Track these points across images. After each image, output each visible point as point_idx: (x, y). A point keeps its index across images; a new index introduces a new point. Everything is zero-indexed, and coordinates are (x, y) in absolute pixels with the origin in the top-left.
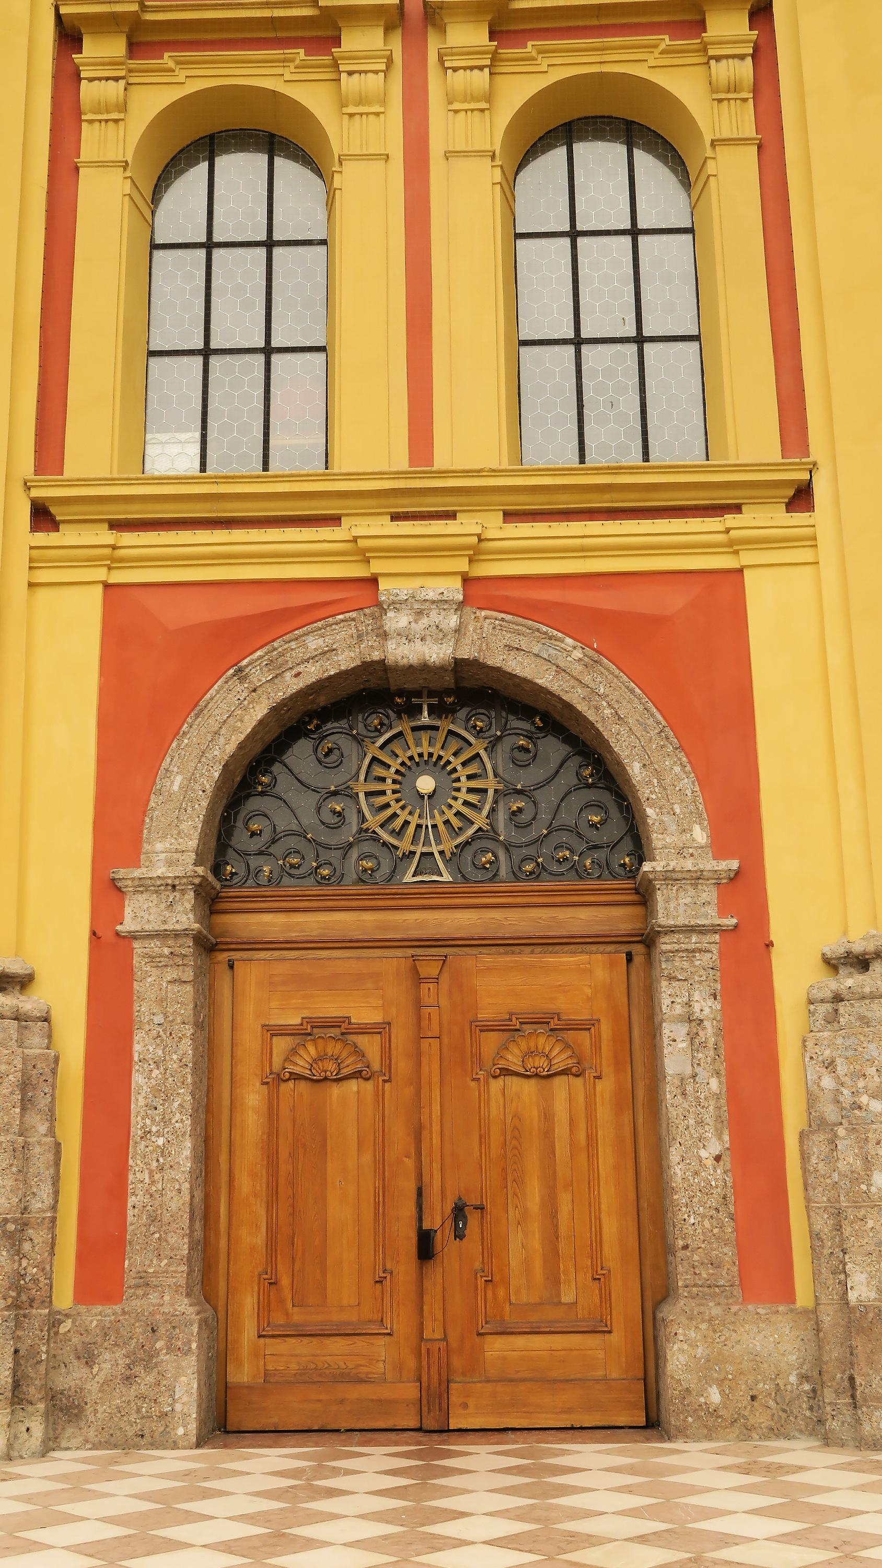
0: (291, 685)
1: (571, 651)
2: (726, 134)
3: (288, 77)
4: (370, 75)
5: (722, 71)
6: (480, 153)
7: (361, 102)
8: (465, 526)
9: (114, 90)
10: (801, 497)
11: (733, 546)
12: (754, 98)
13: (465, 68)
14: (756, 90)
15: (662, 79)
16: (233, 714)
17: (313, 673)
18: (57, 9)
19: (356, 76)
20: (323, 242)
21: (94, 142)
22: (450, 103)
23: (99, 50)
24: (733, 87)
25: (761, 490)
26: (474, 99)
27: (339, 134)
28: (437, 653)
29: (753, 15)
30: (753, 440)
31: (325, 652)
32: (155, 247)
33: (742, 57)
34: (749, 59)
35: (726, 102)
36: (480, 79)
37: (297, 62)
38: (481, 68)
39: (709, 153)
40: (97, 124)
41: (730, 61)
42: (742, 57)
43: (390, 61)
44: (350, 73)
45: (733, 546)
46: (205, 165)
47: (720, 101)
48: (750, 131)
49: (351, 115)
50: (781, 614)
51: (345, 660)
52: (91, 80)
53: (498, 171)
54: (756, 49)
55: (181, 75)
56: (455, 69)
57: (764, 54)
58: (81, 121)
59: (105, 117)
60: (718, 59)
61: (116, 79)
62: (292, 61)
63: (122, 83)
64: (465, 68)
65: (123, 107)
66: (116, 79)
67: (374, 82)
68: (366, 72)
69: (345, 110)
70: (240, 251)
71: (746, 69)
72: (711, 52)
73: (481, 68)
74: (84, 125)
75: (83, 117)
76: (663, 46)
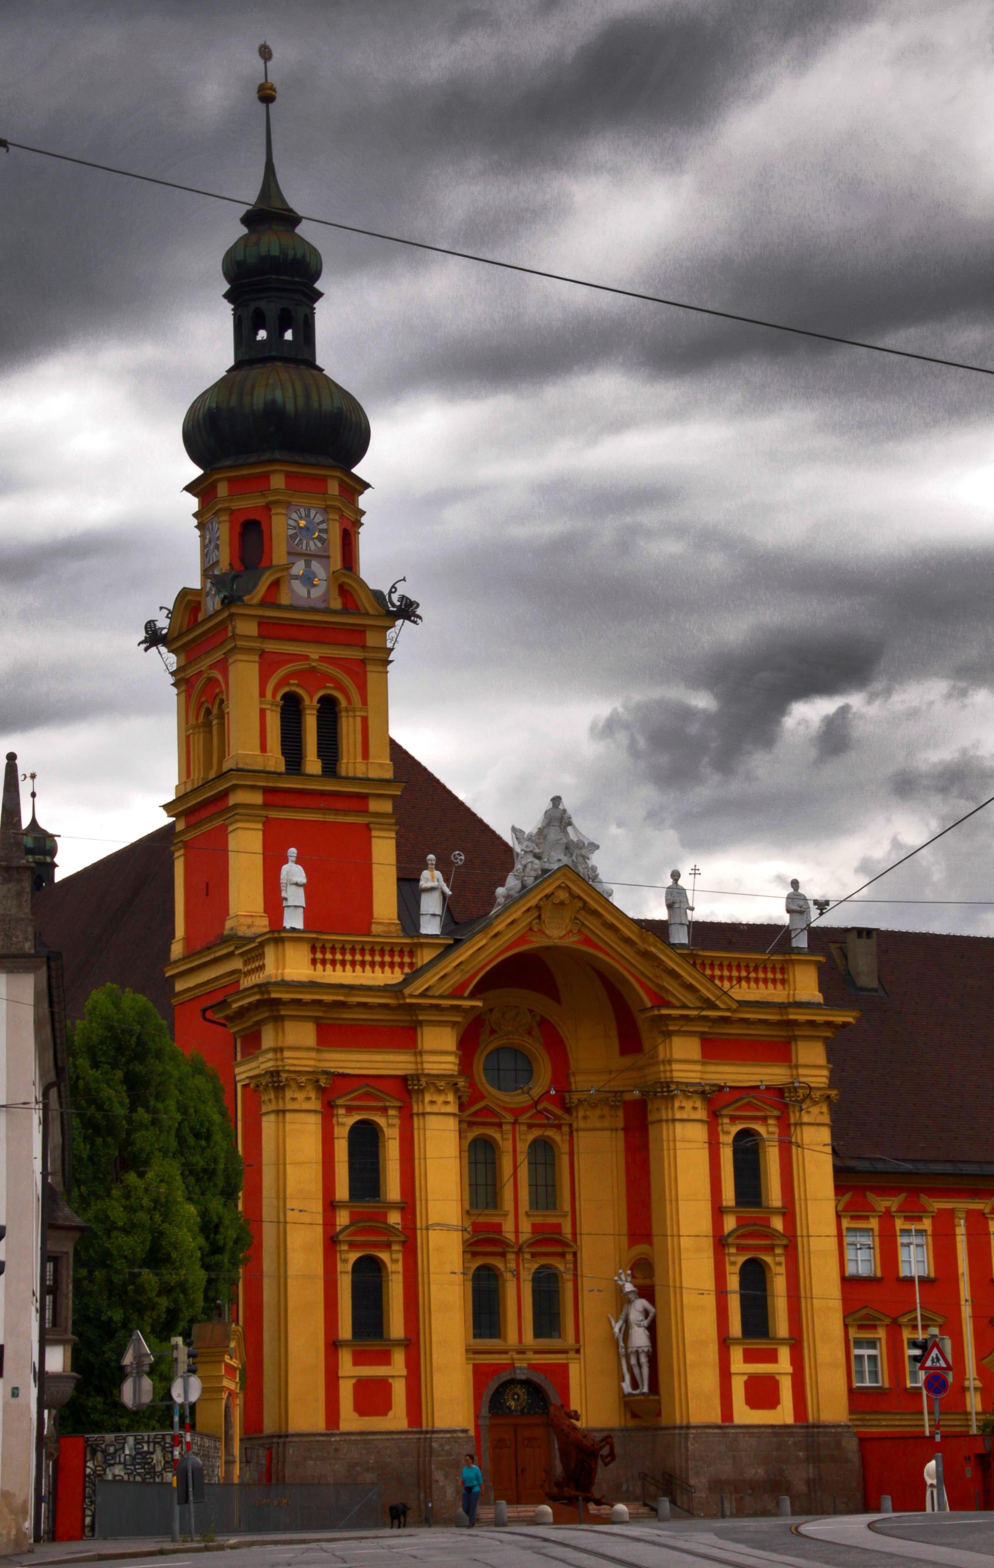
0: (501, 1381)
1: (543, 1377)
8: (530, 1355)
10: (578, 1351)
11: (567, 1359)
15: (558, 1265)
16: (493, 1385)
17: (504, 1379)
25: (571, 1349)
28: (523, 1377)
30: (571, 1339)
31: (505, 1376)
45: (567, 1359)
50: (574, 1371)
51: (509, 1378)
57: (575, 1262)
71: (571, 1266)
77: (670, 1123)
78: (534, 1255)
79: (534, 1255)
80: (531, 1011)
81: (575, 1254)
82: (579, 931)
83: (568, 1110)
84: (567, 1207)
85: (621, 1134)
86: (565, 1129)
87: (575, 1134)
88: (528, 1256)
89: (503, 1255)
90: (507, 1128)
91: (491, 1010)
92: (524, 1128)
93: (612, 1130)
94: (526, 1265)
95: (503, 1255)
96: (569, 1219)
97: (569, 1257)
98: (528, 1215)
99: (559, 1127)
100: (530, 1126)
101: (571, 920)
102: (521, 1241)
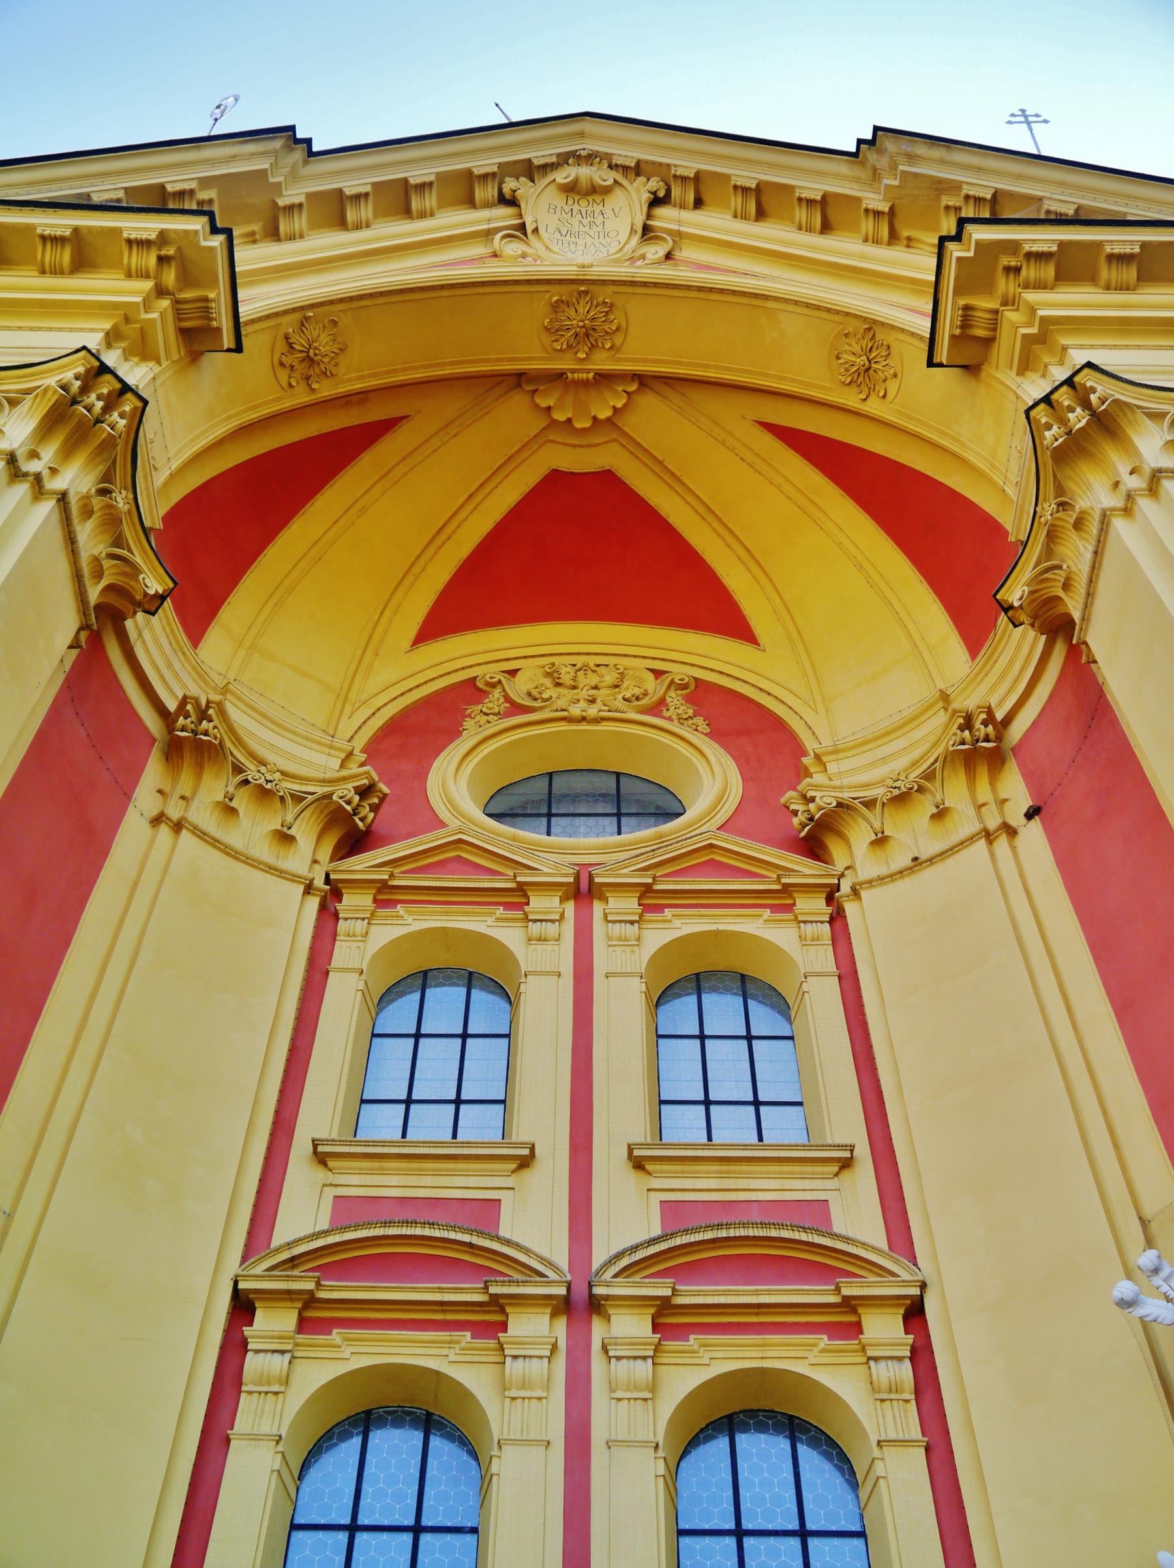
2: (892, 1435)
3: (453, 1357)
4: (534, 1360)
5: (882, 1372)
6: (642, 1444)
7: (523, 1386)
9: (278, 1363)
12: (917, 1400)
13: (628, 1358)
14: (918, 1392)
15: (822, 1376)
18: (236, 1283)
19: (521, 1360)
20: (474, 1530)
21: (252, 1415)
22: (613, 1391)
23: (272, 1323)
24: (894, 1388)
26: (637, 1388)
27: (499, 1418)
29: (906, 1319)
32: (294, 1527)
33: (900, 1359)
34: (908, 1361)
35: (888, 1403)
36: (643, 1370)
37: (463, 1344)
38: (644, 1358)
39: (876, 1453)
40: (257, 1395)
41: (889, 1362)
42: (900, 1359)
43: (555, 1347)
44: (515, 1357)
46: (357, 1441)
47: (882, 1401)
48: (915, 1432)
49: (513, 1399)
52: (257, 1351)
53: (661, 1463)
54: (914, 1350)
55: (347, 1351)
56: (618, 1358)
57: (921, 1356)
58: (240, 1392)
59: (265, 1389)
60: (876, 1359)
61: (283, 1352)
62: (458, 1342)
63: (287, 1356)
64: (628, 1358)
65: (286, 1381)
66: (283, 1352)
67: (537, 1368)
68: (531, 1357)
69: (507, 1393)
70: (385, 1536)
71: (905, 1372)
72: (870, 1353)
73: (644, 1358)
74: (243, 1396)
75: (244, 1388)
76: (822, 1345)
77: (1144, 504)
78: (669, 1321)
79: (669, 1321)
80: (658, 673)
81: (914, 1313)
82: (668, 256)
83: (813, 845)
84: (846, 1125)
85: (1033, 834)
86: (813, 906)
87: (851, 909)
88: (631, 1326)
89: (489, 1321)
90: (538, 903)
91: (513, 673)
92: (629, 904)
93: (989, 836)
94: (622, 1369)
95: (489, 1321)
96: (865, 1173)
97: (884, 1328)
98: (639, 1164)
99: (781, 900)
100: (651, 900)
101: (633, 231)
102: (598, 1260)
